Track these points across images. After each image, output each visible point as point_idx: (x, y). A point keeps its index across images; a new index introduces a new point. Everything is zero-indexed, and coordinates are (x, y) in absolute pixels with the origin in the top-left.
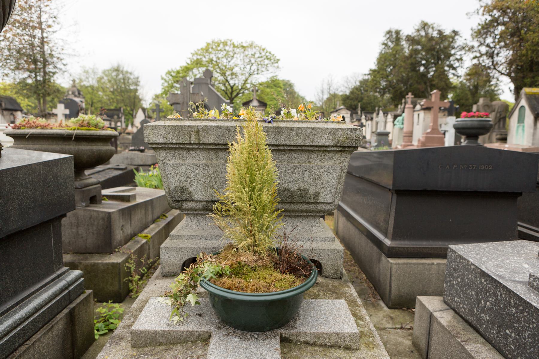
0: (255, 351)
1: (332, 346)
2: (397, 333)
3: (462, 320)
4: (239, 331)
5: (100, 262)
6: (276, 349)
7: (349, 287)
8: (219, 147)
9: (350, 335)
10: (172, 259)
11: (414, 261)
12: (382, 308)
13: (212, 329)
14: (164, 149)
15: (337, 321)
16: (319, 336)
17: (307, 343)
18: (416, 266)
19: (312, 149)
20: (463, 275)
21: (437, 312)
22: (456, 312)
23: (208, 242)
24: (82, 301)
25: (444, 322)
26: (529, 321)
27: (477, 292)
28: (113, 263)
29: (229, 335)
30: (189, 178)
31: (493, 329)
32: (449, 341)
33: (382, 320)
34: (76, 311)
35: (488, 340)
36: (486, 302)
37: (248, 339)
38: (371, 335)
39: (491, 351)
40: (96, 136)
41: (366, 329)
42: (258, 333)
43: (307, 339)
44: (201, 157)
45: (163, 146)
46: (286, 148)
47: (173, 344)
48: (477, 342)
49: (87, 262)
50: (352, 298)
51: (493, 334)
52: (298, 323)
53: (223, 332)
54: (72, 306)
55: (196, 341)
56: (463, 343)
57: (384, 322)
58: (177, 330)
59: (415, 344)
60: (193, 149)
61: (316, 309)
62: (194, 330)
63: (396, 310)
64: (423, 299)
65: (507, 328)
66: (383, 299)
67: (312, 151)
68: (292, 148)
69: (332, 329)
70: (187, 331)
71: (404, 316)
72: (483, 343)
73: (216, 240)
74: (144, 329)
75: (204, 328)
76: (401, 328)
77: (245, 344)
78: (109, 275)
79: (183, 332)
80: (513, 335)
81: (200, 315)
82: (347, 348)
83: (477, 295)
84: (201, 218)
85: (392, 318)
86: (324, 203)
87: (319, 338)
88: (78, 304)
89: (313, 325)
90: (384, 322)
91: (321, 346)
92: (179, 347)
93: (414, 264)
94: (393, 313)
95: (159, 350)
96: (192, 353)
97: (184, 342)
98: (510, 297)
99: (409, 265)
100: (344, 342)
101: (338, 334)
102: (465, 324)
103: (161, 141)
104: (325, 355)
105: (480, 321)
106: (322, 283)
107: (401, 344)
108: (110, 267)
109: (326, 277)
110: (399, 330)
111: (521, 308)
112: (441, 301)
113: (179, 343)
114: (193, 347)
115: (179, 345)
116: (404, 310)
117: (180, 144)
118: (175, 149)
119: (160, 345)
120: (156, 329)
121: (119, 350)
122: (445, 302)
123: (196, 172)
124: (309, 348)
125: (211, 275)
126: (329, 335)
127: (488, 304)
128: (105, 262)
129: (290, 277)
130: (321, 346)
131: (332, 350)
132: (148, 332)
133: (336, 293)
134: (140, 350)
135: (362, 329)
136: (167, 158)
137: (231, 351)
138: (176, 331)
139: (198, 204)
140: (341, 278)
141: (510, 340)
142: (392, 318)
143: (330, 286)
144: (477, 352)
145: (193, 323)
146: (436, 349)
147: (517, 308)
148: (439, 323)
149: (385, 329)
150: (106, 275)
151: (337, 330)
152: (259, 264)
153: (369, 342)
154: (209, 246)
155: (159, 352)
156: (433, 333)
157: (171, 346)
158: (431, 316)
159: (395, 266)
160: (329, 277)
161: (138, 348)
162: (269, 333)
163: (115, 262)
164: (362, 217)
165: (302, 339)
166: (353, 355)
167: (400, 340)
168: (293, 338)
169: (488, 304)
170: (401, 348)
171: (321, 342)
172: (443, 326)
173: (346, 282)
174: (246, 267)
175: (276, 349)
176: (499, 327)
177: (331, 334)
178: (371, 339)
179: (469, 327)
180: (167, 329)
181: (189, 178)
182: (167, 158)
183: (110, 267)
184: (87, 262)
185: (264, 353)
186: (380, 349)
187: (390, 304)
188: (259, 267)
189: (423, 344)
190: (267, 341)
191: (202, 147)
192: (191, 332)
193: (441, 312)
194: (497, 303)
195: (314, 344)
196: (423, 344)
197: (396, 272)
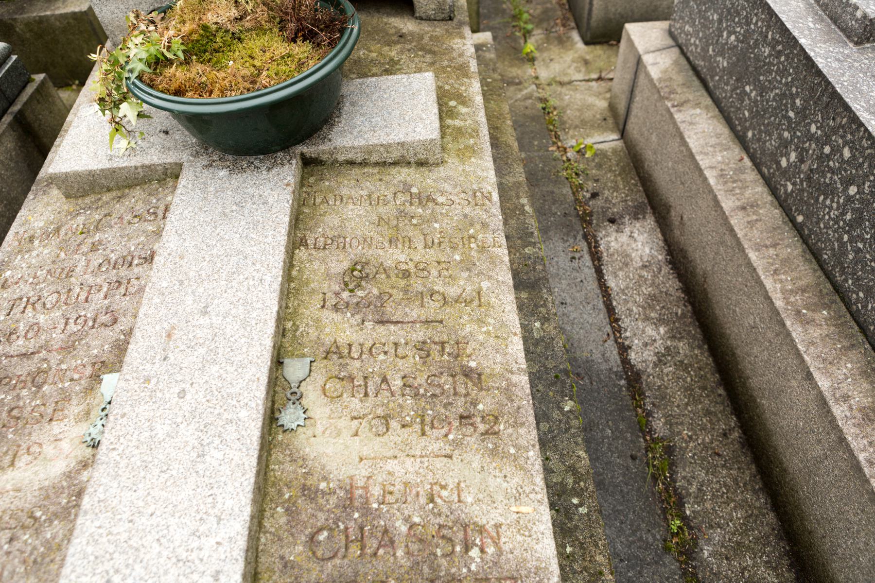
0: (250, 191)
1: (395, 163)
2: (589, 89)
3: (687, 67)
4: (230, 157)
5: (48, 13)
6: (288, 185)
7: (463, 37)
9: (424, 143)
10: (121, 15)
12: (573, 44)
13: (184, 157)
15: (407, 119)
16: (369, 150)
17: (351, 163)
21: (651, 54)
22: (683, 53)
24: (32, 97)
25: (655, 73)
26: (783, 73)
27: (721, 15)
28: (74, 13)
29: (211, 166)
31: (727, 84)
32: (656, 106)
33: (569, 67)
34: (28, 113)
35: (717, 102)
36: (730, 34)
37: (243, 170)
38: (476, 132)
39: (715, 121)
41: (469, 121)
42: (262, 157)
43: (350, 156)
47: (130, 187)
48: (698, 105)
49: (25, 16)
50: (460, 61)
51: (725, 91)
52: (336, 129)
53: (204, 160)
54: (16, 108)
55: (165, 179)
56: (673, 110)
57: (571, 71)
58: (124, 165)
59: (612, 108)
61: (374, 97)
62: (153, 162)
63: (598, 47)
64: (633, 29)
65: (748, 83)
66: (578, 27)
69: (391, 137)
70: (142, 166)
71: (608, 57)
72: (707, 108)
74: (69, 170)
75: (170, 158)
76: (600, 79)
77: (237, 179)
78: (77, 37)
79: (136, 168)
80: (753, 94)
81: (166, 133)
82: (421, 164)
83: (720, 21)
85: (586, 62)
87: (370, 153)
88: (26, 104)
89: (360, 131)
90: (571, 71)
91: (377, 164)
92: (137, 192)
94: (592, 52)
95: (108, 199)
96: (158, 200)
97: (146, 183)
98: (769, 27)
100: (415, 155)
101: (402, 144)
102: (691, 73)
104: (381, 180)
105: (712, 70)
106: (412, 34)
107: (589, 107)
108: (71, 21)
109: (421, 19)
110: (594, 84)
111: (780, 48)
112: (662, 29)
113: (137, 185)
114: (160, 189)
115: (138, 188)
116: (612, 45)
119: (109, 190)
120: (90, 168)
121: (48, 204)
122: (671, 34)
124: (355, 171)
125: (140, 67)
126: (387, 147)
127: (733, 38)
128: (57, 12)
129: (301, 49)
130: (377, 164)
131: (394, 171)
132: (77, 175)
133: (434, 53)
134: (80, 201)
135: (462, 123)
137: (211, 197)
138: (123, 168)
140: (451, 19)
141: (747, 102)
142: (586, 62)
143: (426, 39)
144: (691, 123)
145: (153, 150)
146: (636, 116)
147: (773, 48)
148: (648, 75)
149: (570, 83)
150: (71, 37)
151: (401, 136)
152: (248, 25)
153: (466, 147)
155: (107, 203)
156: (637, 92)
157: (127, 191)
158: (639, 61)
160: (428, 19)
161: (76, 198)
162: (280, 154)
163: (77, 10)
165: (341, 158)
166: (431, 174)
167: (591, 100)
168: (325, 157)
169: (733, 38)
170: (588, 115)
171: (374, 158)
172: (651, 80)
173: (461, 24)
174: (220, 34)
175: (288, 185)
176: (737, 80)
177: (390, 145)
178: (472, 141)
179: (695, 78)
180: (108, 165)
183: (71, 21)
184: (25, 16)
186: (481, 159)
187: (589, 35)
188: (248, 30)
189: (622, 108)
190: (274, 171)
192: (149, 167)
193: (658, 53)
194: (745, 39)
195: (364, 164)
196: (622, 108)
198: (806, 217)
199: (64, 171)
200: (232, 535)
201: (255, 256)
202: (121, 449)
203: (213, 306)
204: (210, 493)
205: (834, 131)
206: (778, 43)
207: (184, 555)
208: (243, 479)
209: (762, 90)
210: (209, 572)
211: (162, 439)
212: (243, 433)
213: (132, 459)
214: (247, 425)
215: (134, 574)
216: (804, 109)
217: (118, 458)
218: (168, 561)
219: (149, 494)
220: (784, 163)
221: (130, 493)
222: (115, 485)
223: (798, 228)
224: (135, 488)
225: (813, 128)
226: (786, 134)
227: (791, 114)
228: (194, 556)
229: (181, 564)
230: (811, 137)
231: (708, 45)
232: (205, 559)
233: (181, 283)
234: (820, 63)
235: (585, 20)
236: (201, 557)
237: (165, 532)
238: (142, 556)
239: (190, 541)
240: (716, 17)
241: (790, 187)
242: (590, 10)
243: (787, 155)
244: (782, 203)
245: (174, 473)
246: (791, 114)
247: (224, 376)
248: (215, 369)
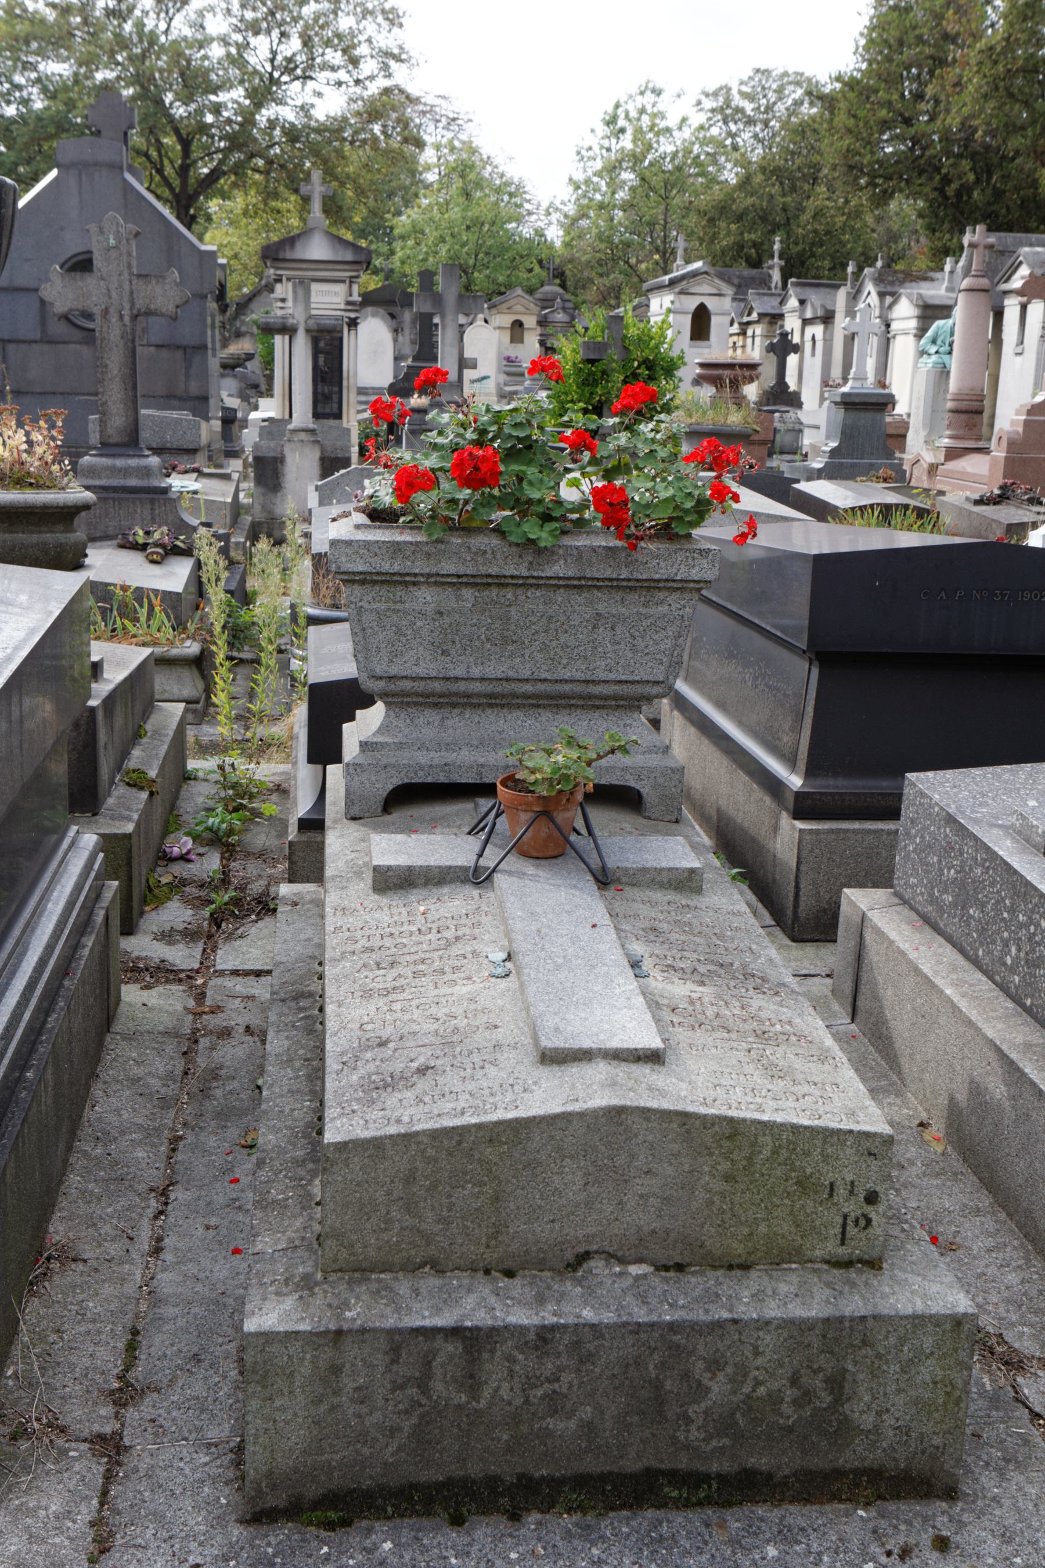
8: (465, 580)
11: (856, 825)
14: (363, 582)
18: (859, 837)
19: (630, 584)
20: (925, 828)
23: (433, 754)
26: (993, 884)
27: (939, 856)
30: (405, 635)
35: (949, 939)
40: (57, 507)
44: (429, 598)
45: (362, 577)
46: (583, 582)
51: (954, 924)
60: (414, 584)
67: (630, 588)
68: (595, 583)
73: (447, 750)
83: (940, 862)
84: (414, 710)
86: (648, 682)
93: (855, 832)
98: (977, 851)
99: (842, 835)
103: (360, 569)
117: (394, 574)
118: (383, 582)
122: (896, 894)
123: (419, 624)
136: (365, 598)
139: (416, 684)
154: (436, 761)
159: (808, 837)
164: (741, 724)
177: (662, 869)
181: (405, 635)
182: (365, 598)
191: (432, 580)
197: (812, 851)
198: (1032, 996)
205: (1032, 911)
206: (985, 860)
209: (982, 905)
216: (1013, 904)
220: (1009, 960)
223: (1028, 1010)
225: (1021, 917)
226: (1006, 934)
227: (1005, 915)
230: (1021, 925)
231: (932, 889)
234: (1016, 865)
235: (789, 912)
240: (935, 859)
241: (1017, 979)
242: (796, 905)
243: (1009, 953)
244: (1017, 1001)
246: (1005, 915)
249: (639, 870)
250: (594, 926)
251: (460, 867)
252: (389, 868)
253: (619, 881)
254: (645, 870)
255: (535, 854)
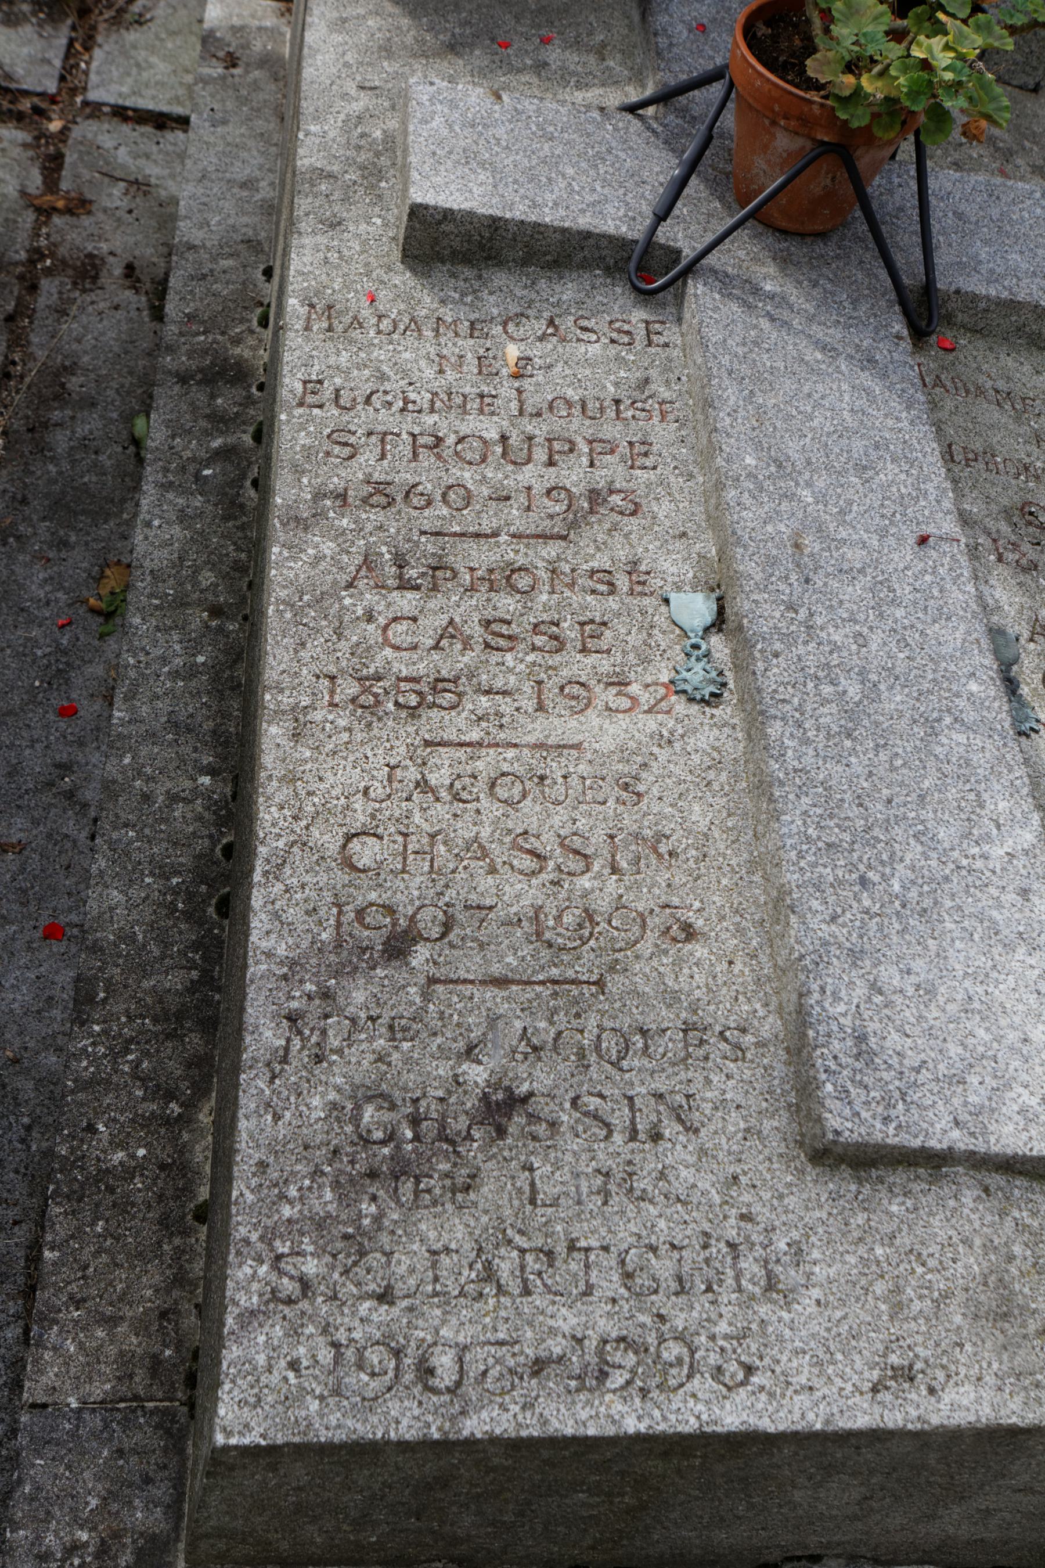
74: (455, 207)
185: (865, 343)
199: (448, 206)
200: (1026, 846)
201: (892, 447)
202: (796, 700)
203: (853, 515)
204: (968, 787)
207: (965, 862)
208: (1011, 777)
210: (1011, 888)
211: (857, 699)
212: (985, 713)
213: (821, 720)
214: (987, 704)
215: (897, 875)
217: (797, 715)
218: (942, 866)
219: (870, 772)
221: (840, 768)
222: (811, 752)
224: (844, 762)
228: (979, 864)
229: (964, 872)
232: (998, 870)
233: (780, 466)
236: (991, 867)
237: (920, 827)
238: (899, 854)
239: (965, 846)
245: (900, 751)
247: (920, 627)
248: (899, 613)
249: (1000, 303)
250: (923, 540)
251: (610, 239)
252: (448, 215)
253: (949, 319)
254: (1012, 305)
255: (784, 224)
